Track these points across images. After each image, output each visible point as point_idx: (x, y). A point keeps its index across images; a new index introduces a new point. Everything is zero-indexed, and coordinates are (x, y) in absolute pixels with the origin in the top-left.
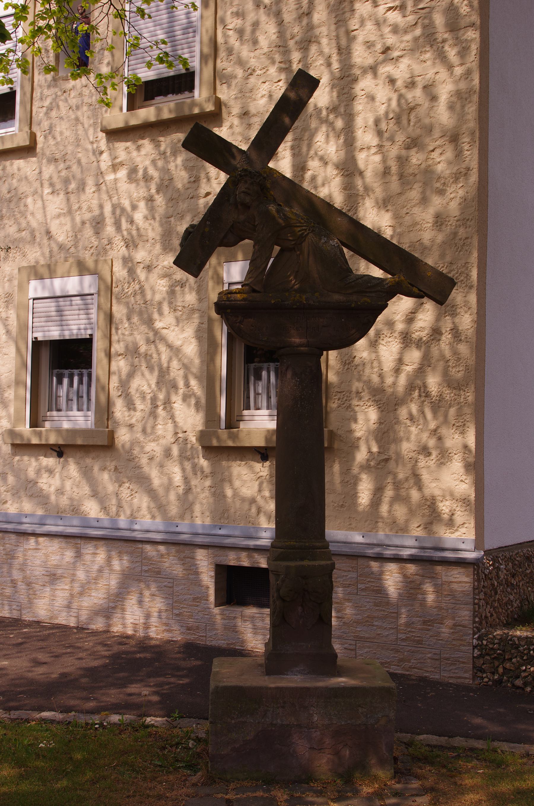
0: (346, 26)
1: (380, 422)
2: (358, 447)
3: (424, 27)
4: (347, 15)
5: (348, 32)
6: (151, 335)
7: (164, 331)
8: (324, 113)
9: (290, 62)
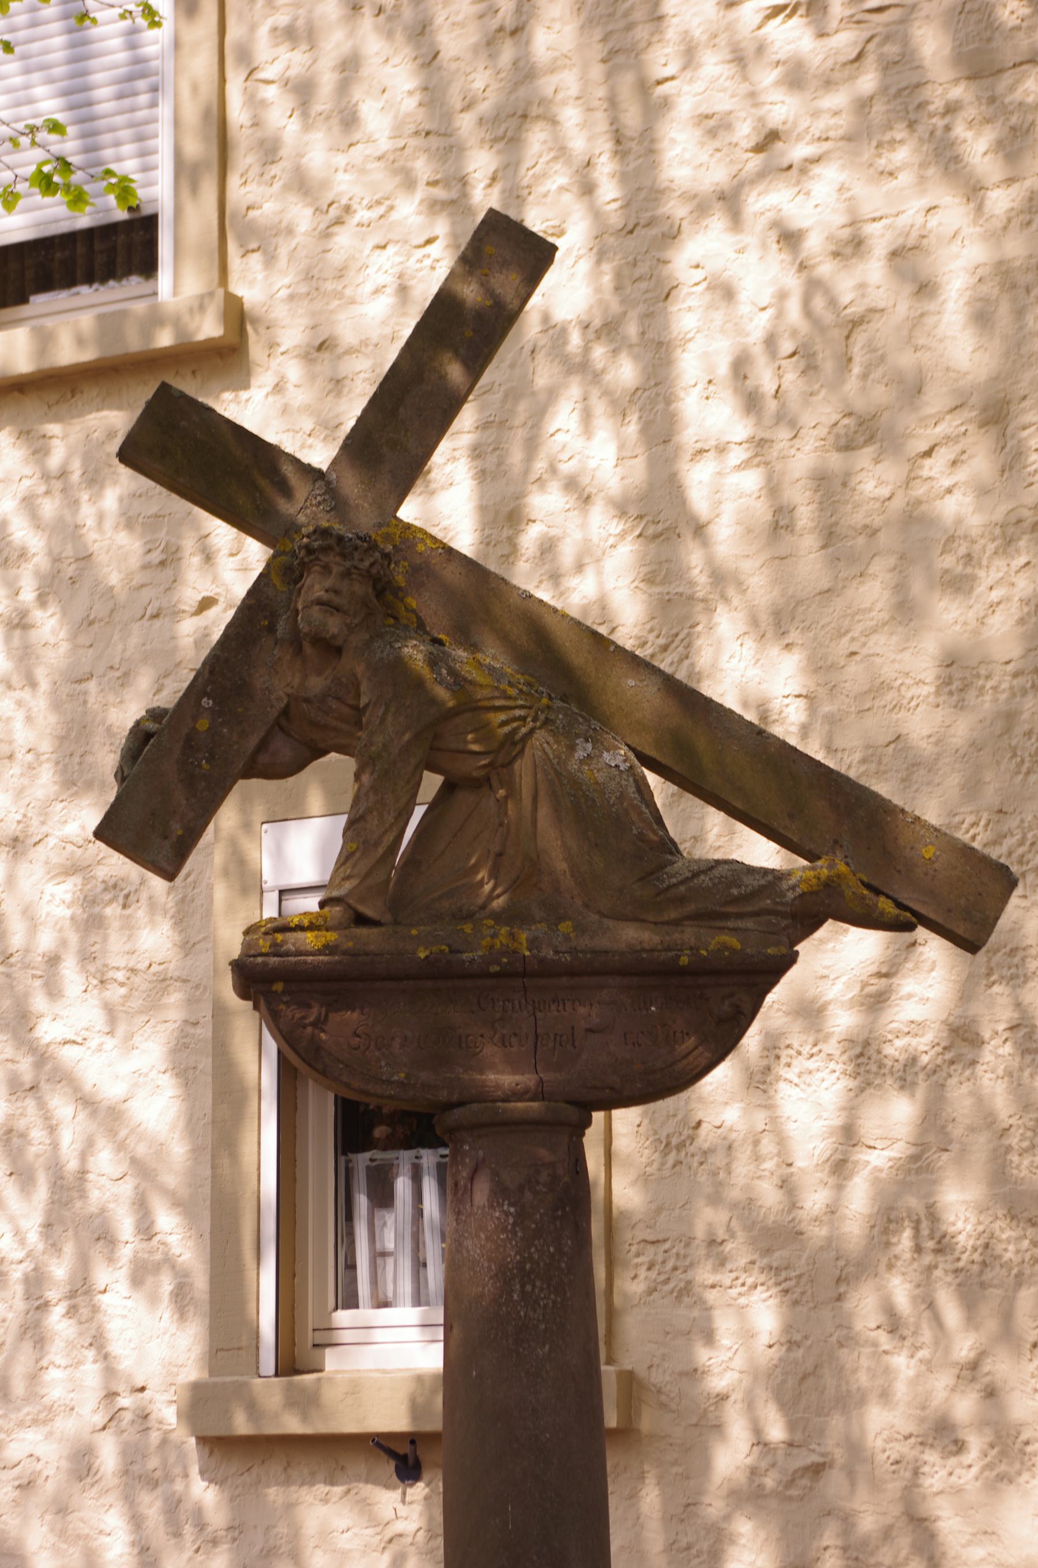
0: (639, 66)
1: (791, 1339)
2: (718, 1428)
3: (887, 66)
4: (641, 33)
5: (644, 87)
6: (25, 1066)
7: (69, 1053)
8: (575, 340)
9: (463, 181)
